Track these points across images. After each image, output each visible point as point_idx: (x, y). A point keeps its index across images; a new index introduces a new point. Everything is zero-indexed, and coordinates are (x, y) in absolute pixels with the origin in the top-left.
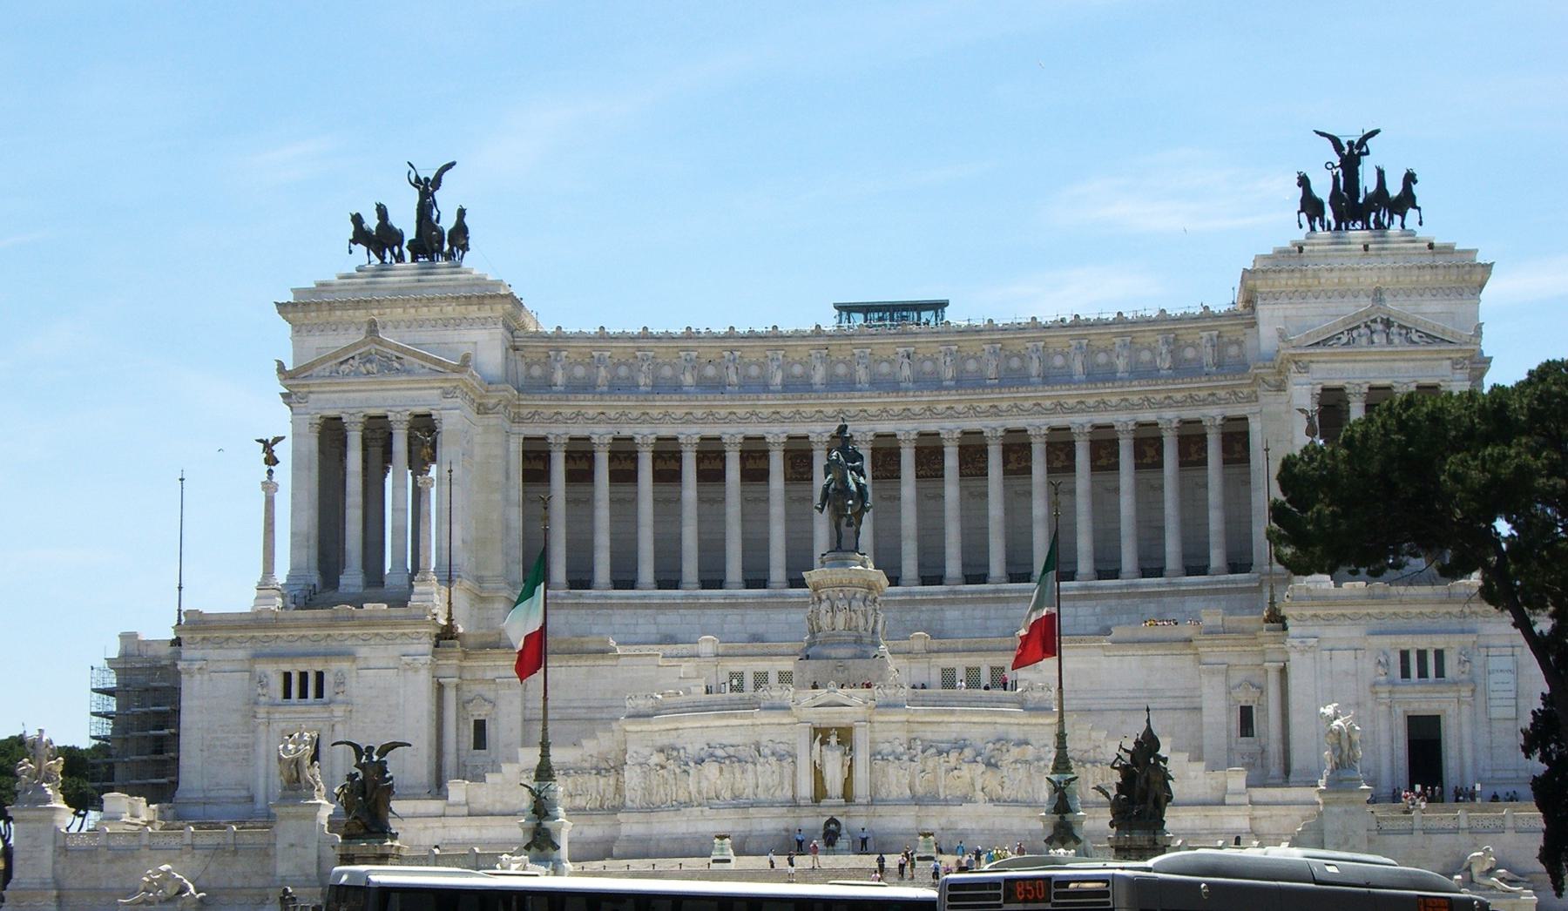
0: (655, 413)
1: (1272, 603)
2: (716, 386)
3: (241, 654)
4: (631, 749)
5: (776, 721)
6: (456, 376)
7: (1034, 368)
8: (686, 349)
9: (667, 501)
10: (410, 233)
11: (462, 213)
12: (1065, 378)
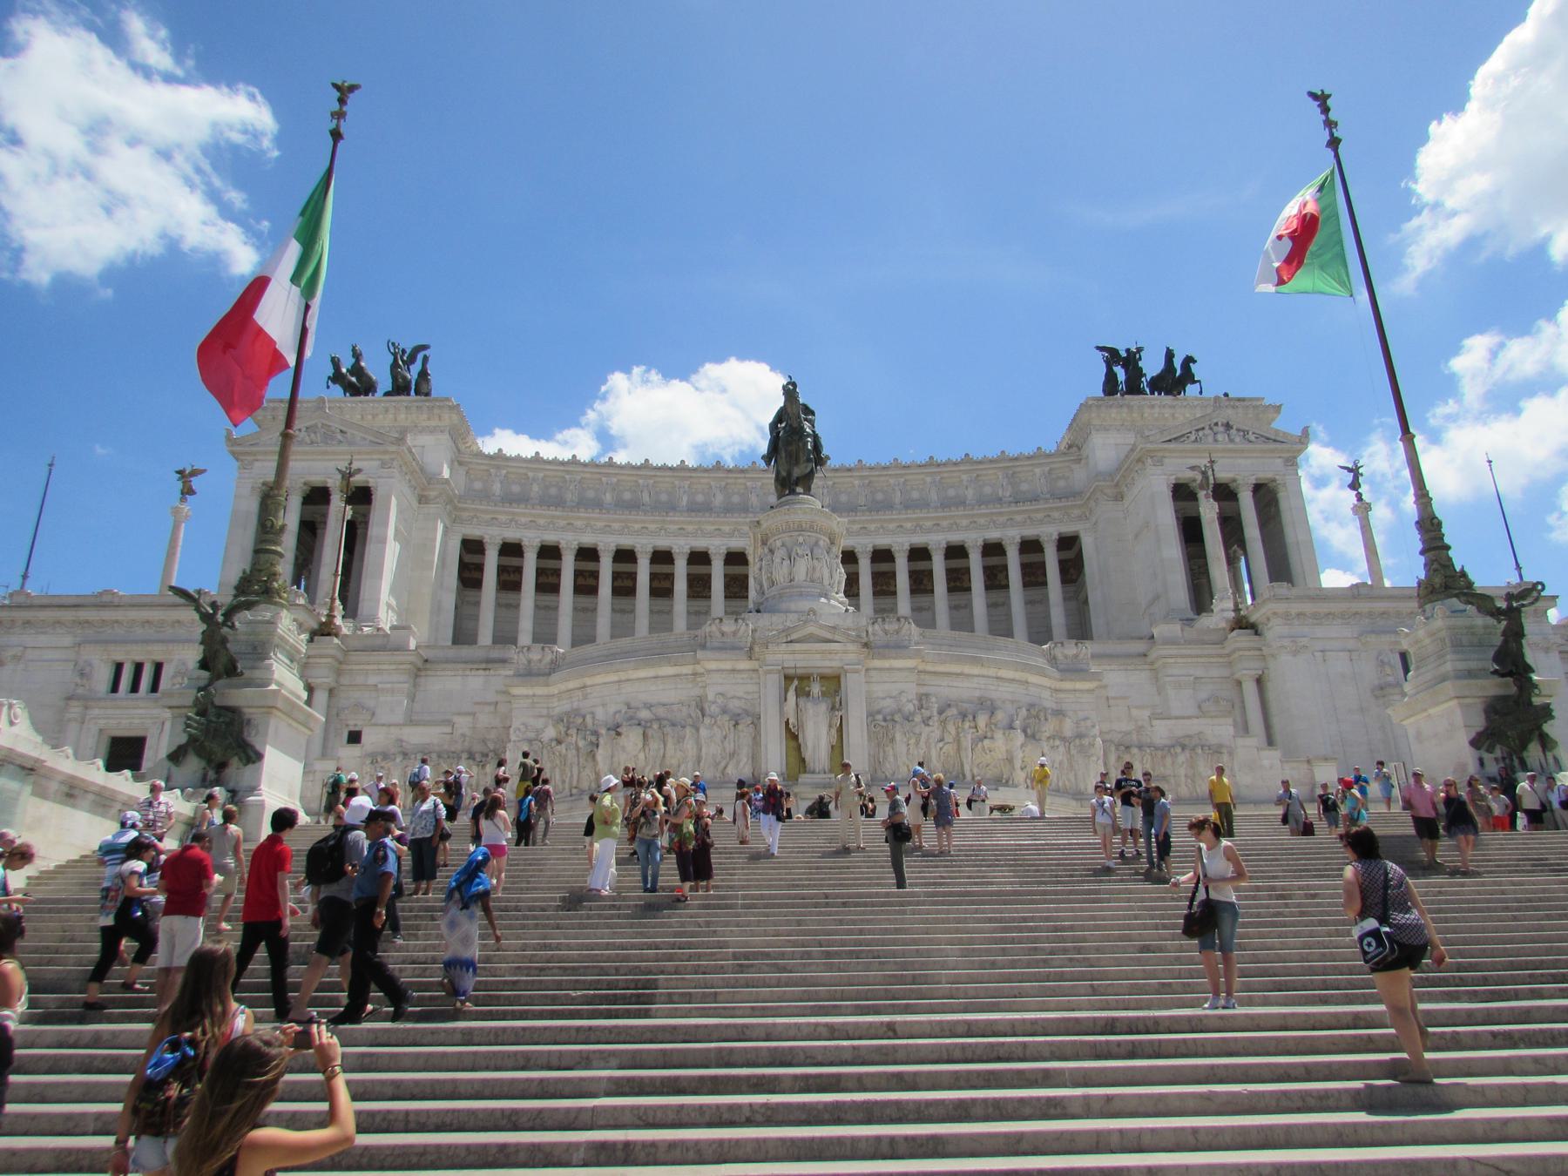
0: (579, 523)
1: (1237, 609)
2: (634, 506)
3: (68, 640)
4: (516, 724)
5: (728, 665)
6: (393, 448)
7: (897, 498)
8: (607, 475)
9: (585, 610)
10: (384, 382)
11: (426, 359)
12: (923, 504)
